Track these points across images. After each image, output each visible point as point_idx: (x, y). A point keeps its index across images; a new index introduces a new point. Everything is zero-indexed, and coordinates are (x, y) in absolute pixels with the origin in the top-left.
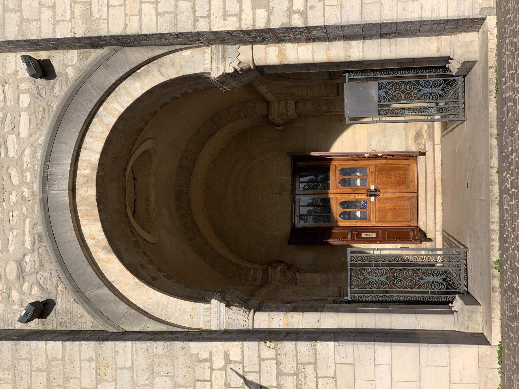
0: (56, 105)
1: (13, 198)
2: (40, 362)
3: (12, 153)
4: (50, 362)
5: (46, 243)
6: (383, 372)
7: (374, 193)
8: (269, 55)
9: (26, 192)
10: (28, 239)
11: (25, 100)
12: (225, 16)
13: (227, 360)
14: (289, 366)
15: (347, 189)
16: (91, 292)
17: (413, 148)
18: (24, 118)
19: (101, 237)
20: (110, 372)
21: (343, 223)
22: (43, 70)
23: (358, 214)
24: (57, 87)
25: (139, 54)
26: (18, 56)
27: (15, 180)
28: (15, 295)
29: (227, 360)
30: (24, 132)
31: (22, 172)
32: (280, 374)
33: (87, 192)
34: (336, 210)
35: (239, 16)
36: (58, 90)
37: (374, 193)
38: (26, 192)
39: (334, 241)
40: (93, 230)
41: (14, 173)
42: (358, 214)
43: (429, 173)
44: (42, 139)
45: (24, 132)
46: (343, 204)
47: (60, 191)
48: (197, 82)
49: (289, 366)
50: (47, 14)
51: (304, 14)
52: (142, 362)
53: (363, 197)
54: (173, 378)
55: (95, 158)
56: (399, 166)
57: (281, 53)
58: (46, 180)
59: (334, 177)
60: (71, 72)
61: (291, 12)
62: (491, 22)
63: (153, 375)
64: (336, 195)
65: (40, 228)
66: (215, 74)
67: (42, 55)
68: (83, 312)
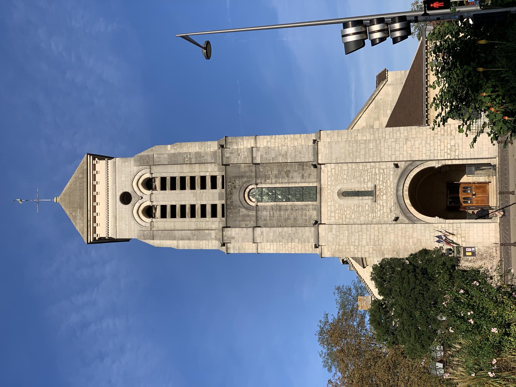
0: (399, 174)
1: (389, 194)
2: (400, 228)
3: (389, 185)
4: (402, 228)
5: (397, 204)
6: (475, 229)
7: (474, 195)
8: (449, 163)
9: (392, 193)
10: (392, 204)
11: (392, 173)
12: (441, 156)
13: (442, 227)
14: (455, 228)
15: (465, 194)
16: (408, 215)
17: (487, 181)
18: (391, 176)
19: (410, 203)
20: (416, 230)
21: (464, 205)
22: (397, 166)
23: (469, 202)
24: (399, 170)
25: (420, 163)
26: (393, 163)
27: (389, 190)
28: (389, 216)
29: (442, 227)
30: (391, 180)
31: (391, 189)
32: (453, 230)
33: (406, 193)
34: (462, 200)
35: (444, 156)
36: (400, 170)
37: (474, 195)
38: (392, 193)
39: (461, 210)
40: (408, 201)
41: (389, 189)
42: (469, 202)
43: (493, 189)
44: (396, 181)
45: (391, 180)
46: (464, 198)
47: (400, 193)
48: (433, 168)
49: (455, 228)
50: (401, 156)
51: (458, 156)
52: (423, 228)
53: (471, 196)
54: (430, 231)
55: (408, 185)
56: (483, 187)
57: (452, 162)
58: (397, 190)
59: (461, 190)
60: (402, 166)
61: (455, 156)
62: (497, 158)
63: (425, 231)
64: (462, 196)
65: (396, 201)
66: (436, 167)
67: (396, 163)
68: (406, 219)
